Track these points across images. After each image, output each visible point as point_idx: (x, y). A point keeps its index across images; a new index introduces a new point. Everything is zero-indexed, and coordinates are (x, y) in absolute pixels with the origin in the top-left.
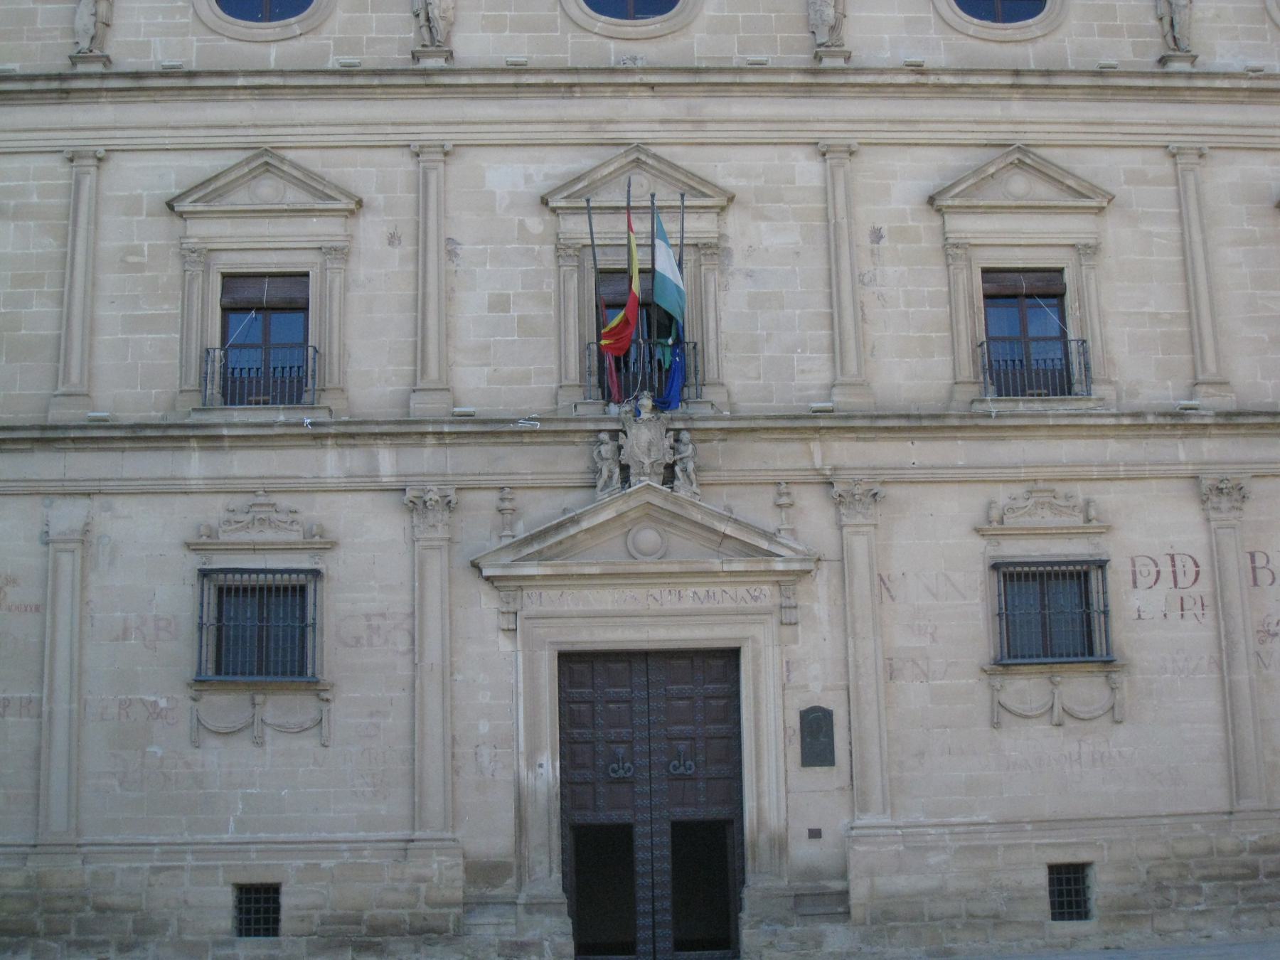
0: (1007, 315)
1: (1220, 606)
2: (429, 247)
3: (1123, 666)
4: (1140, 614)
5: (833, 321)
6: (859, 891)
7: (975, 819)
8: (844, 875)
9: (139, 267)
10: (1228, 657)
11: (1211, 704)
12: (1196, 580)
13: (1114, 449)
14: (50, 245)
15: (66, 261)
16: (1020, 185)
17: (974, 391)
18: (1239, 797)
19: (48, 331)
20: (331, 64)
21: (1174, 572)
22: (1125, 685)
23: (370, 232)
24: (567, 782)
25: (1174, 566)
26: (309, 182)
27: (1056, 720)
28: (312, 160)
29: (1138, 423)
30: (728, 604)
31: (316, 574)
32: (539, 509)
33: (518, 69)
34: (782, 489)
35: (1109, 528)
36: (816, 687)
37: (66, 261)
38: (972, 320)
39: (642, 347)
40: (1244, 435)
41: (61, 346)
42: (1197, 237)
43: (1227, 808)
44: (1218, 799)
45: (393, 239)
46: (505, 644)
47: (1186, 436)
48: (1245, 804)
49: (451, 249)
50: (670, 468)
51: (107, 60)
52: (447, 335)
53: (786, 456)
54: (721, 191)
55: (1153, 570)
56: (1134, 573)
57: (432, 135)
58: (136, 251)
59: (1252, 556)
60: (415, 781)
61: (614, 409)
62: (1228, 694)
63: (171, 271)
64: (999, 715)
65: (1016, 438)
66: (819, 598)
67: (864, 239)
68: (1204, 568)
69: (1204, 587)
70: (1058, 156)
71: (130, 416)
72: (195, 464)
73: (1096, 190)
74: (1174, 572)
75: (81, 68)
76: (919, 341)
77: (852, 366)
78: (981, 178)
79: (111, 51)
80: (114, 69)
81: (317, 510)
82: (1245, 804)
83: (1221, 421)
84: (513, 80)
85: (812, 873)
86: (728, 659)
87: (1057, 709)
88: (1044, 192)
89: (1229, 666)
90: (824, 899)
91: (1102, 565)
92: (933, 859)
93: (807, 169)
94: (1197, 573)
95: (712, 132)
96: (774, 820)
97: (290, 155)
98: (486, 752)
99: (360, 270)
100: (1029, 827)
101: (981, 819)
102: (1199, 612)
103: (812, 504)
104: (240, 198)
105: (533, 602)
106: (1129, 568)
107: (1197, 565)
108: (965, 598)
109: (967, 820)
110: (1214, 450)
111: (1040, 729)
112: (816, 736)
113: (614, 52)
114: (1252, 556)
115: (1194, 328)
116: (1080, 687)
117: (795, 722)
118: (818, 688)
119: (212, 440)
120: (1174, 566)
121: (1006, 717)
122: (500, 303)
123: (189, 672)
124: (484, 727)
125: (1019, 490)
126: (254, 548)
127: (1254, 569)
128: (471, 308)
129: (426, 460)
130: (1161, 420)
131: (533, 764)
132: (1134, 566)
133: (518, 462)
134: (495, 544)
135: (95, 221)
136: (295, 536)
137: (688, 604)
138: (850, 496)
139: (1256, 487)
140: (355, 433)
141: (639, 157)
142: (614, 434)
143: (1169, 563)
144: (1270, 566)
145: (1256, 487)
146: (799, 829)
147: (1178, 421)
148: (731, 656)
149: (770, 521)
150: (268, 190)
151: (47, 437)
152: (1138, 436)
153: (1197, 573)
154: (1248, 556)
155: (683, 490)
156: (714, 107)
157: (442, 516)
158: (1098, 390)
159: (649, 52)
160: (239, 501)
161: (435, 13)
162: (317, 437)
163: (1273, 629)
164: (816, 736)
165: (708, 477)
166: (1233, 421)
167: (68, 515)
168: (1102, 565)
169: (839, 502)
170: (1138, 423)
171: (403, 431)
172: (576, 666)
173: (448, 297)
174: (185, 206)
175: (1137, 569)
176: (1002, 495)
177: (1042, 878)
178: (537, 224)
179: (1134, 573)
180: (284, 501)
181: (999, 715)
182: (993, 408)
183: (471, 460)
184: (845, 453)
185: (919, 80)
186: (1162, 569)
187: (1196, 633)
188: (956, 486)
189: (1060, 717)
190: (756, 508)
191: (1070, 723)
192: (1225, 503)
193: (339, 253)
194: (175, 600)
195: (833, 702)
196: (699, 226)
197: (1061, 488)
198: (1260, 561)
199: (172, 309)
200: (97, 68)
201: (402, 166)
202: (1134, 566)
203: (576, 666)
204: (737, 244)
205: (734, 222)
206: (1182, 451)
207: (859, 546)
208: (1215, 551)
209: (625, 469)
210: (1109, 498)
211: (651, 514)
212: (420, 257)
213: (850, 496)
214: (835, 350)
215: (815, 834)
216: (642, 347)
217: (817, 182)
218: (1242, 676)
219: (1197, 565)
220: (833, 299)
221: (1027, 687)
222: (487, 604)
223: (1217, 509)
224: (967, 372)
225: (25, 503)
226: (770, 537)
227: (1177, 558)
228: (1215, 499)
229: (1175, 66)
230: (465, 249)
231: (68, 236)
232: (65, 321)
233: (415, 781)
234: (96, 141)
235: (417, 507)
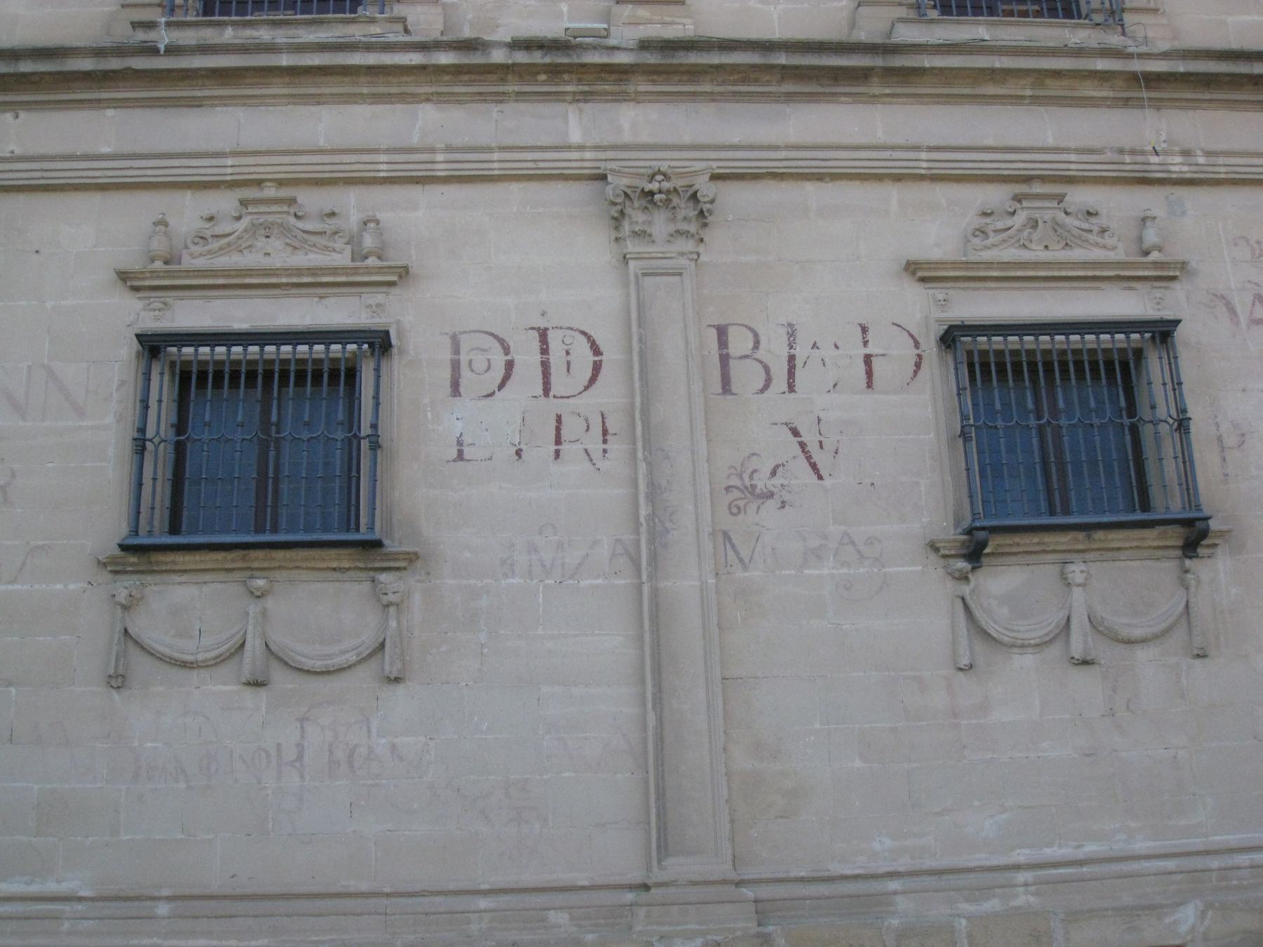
1: (644, 433)
3: (413, 558)
4: (452, 449)
7: (51, 887)
10: (652, 541)
11: (612, 643)
12: (593, 380)
13: (429, 124)
18: (664, 849)
21: (545, 366)
22: (417, 599)
25: (545, 351)
27: (247, 675)
35: (404, 273)
40: (712, 97)
43: (636, 876)
44: (618, 855)
47: (585, 97)
48: (678, 867)
55: (499, 360)
56: (456, 366)
59: (722, 332)
62: (653, 619)
65: (225, 101)
68: (611, 355)
69: (610, 394)
74: (545, 366)
82: (678, 867)
83: (651, 59)
87: (254, 646)
89: (654, 558)
94: (597, 367)
100: (163, 909)
101: (64, 887)
102: (596, 446)
106: (446, 355)
107: (596, 351)
108: (80, 412)
109: (34, 889)
110: (644, 125)
111: (220, 687)
114: (722, 332)
116: (315, 606)
120: (545, 351)
121: (140, 664)
125: (225, 202)
127: (724, 360)
130: (521, 57)
132: (456, 351)
143: (536, 345)
144: (760, 354)
145: (734, 197)
152: (482, 97)
153: (597, 367)
154: (713, 333)
163: (762, 482)
166: (679, 66)
170: (473, 70)
175: (464, 358)
176: (187, 212)
179: (456, 366)
186: (518, 358)
187: (586, 492)
188: (97, 198)
189: (264, 669)
191: (281, 679)
192: (660, 224)
197: (311, 200)
198: (739, 343)
202: (456, 351)
206: (576, 126)
208: (638, 321)
210: (412, 217)
218: (686, 582)
219: (596, 351)
221: (193, 604)
223: (642, 235)
227: (553, 337)
228: (640, 217)
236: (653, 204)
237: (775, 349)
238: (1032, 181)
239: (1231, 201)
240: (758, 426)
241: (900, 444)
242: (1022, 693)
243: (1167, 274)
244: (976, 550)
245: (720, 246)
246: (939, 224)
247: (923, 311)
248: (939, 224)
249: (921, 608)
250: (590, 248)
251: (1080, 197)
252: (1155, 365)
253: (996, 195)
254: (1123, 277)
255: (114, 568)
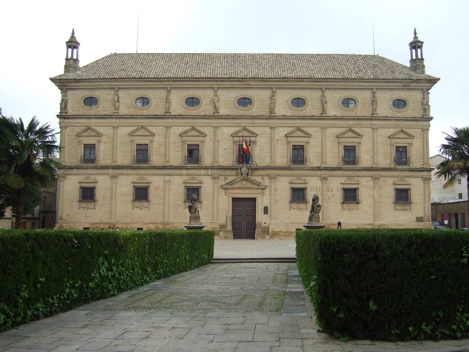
0: (296, 152)
2: (215, 141)
5: (271, 153)
6: (270, 231)
8: (269, 229)
9: (176, 143)
14: (164, 140)
15: (166, 142)
16: (299, 133)
17: (289, 163)
19: (164, 152)
20: (202, 114)
23: (208, 139)
24: (233, 215)
26: (199, 132)
28: (199, 128)
29: (312, 169)
30: (255, 192)
31: (200, 187)
32: (230, 179)
33: (228, 115)
34: (263, 176)
36: (266, 204)
37: (166, 142)
38: (290, 154)
39: (244, 156)
41: (165, 155)
42: (324, 140)
45: (211, 140)
46: (225, 197)
49: (219, 141)
50: (247, 173)
51: (170, 113)
52: (218, 154)
53: (263, 172)
54: (256, 134)
57: (216, 125)
58: (175, 141)
60: (213, 215)
61: (240, 165)
63: (180, 144)
64: (291, 208)
66: (267, 191)
67: (276, 140)
69: (320, 192)
70: (304, 129)
71: (175, 165)
72: (184, 172)
73: (309, 134)
75: (167, 114)
76: (282, 156)
77: (273, 159)
78: (293, 132)
79: (171, 111)
80: (172, 114)
81: (200, 178)
84: (228, 117)
85: (265, 228)
86: (255, 199)
88: (302, 134)
90: (266, 231)
91: (306, 188)
92: (280, 227)
93: (268, 130)
95: (255, 125)
96: (260, 221)
97: (196, 128)
98: (222, 211)
99: (206, 144)
103: (266, 178)
104: (189, 134)
105: (229, 191)
111: (296, 210)
112: (266, 210)
113: (241, 113)
115: (322, 155)
117: (263, 208)
118: (266, 204)
119: (187, 169)
122: (225, 149)
123: (183, 200)
124: (222, 208)
125: (296, 177)
126: (192, 183)
128: (221, 150)
129: (215, 171)
131: (228, 213)
133: (228, 172)
134: (223, 183)
135: (169, 137)
136: (198, 182)
137: (249, 192)
138: (272, 178)
139: (329, 178)
140: (206, 168)
141: (245, 129)
142: (240, 169)
145: (329, 178)
146: (263, 223)
147: (319, 169)
148: (255, 199)
149: (261, 181)
150: (194, 133)
151: (164, 168)
155: (249, 177)
156: (256, 121)
157: (217, 179)
158: (307, 164)
159: (247, 113)
160: (190, 177)
161: (217, 106)
162: (200, 168)
164: (266, 210)
165: (253, 175)
167: (167, 178)
168: (306, 188)
169: (270, 179)
171: (212, 168)
172: (234, 200)
173: (218, 148)
174: (182, 135)
176: (293, 178)
177: (295, 230)
178: (230, 138)
180: (196, 177)
181: (291, 208)
182: (292, 166)
183: (222, 172)
184: (272, 172)
185: (285, 117)
189: (299, 209)
190: (259, 179)
192: (324, 180)
193: (203, 142)
194: (181, 190)
195: (268, 206)
196: (253, 139)
197: (301, 177)
199: (180, 149)
200: (169, 114)
201: (211, 129)
203: (234, 200)
204: (258, 141)
205: (258, 138)
206: (319, 173)
207: (273, 184)
208: (322, 187)
209: (241, 173)
210: (308, 179)
211: (245, 179)
212: (214, 143)
213: (272, 178)
214: (271, 157)
215: (265, 223)
216: (244, 156)
217: (270, 132)
220: (271, 149)
222: (223, 191)
224: (289, 160)
225: (161, 176)
226: (260, 183)
229: (323, 115)
230: (221, 141)
231: (166, 138)
232: (166, 151)
233: (213, 215)
234: (168, 125)
235: (214, 178)
236: (324, 179)
237: (331, 189)
238: (349, 177)
239: (364, 178)
240: (330, 194)
241: (339, 195)
242: (346, 212)
243: (359, 184)
244: (343, 203)
245: (328, 181)
246: (343, 180)
247: (342, 186)
248: (343, 180)
249: (340, 207)
250: (320, 181)
251: (353, 178)
252: (357, 191)
253: (347, 178)
254: (355, 184)
255: (290, 202)
